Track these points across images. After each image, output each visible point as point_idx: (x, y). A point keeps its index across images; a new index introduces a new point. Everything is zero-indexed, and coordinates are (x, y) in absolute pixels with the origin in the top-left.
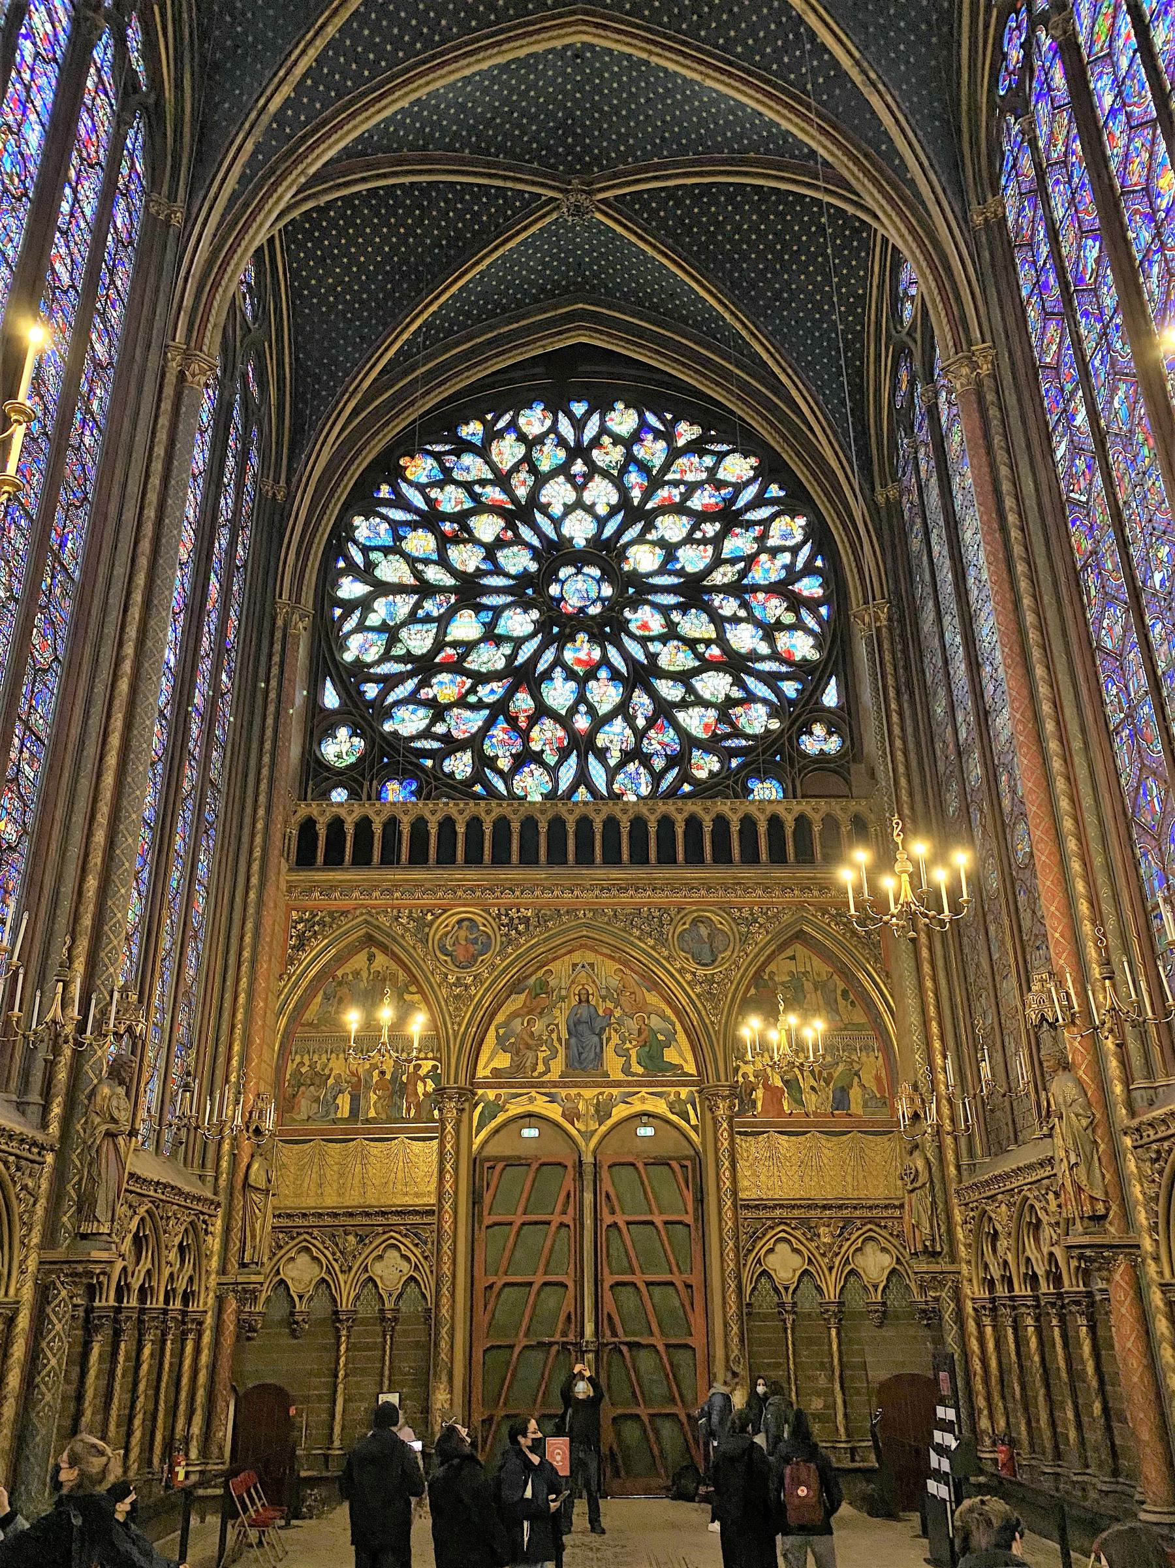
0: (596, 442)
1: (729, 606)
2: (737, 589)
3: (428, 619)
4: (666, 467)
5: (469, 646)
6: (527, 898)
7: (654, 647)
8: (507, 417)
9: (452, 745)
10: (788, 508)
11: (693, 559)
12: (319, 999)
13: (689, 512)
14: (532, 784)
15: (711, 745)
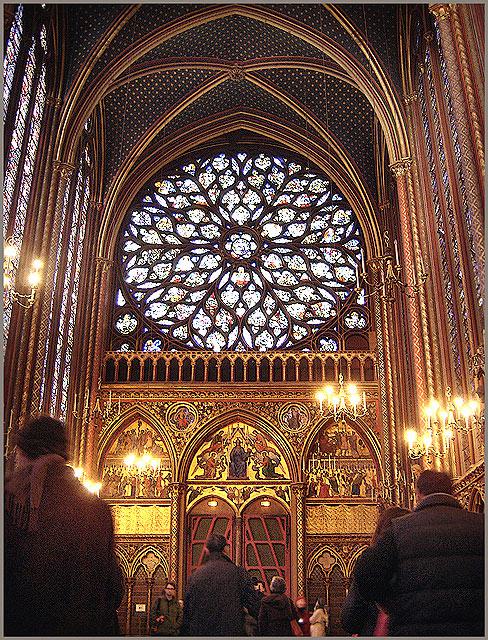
0: (250, 174)
1: (311, 254)
2: (317, 246)
3: (167, 261)
4: (283, 186)
5: (187, 274)
6: (212, 397)
7: (277, 274)
8: (207, 162)
9: (178, 323)
10: (344, 205)
11: (296, 231)
12: (116, 442)
13: (295, 208)
14: (216, 342)
15: (303, 323)
